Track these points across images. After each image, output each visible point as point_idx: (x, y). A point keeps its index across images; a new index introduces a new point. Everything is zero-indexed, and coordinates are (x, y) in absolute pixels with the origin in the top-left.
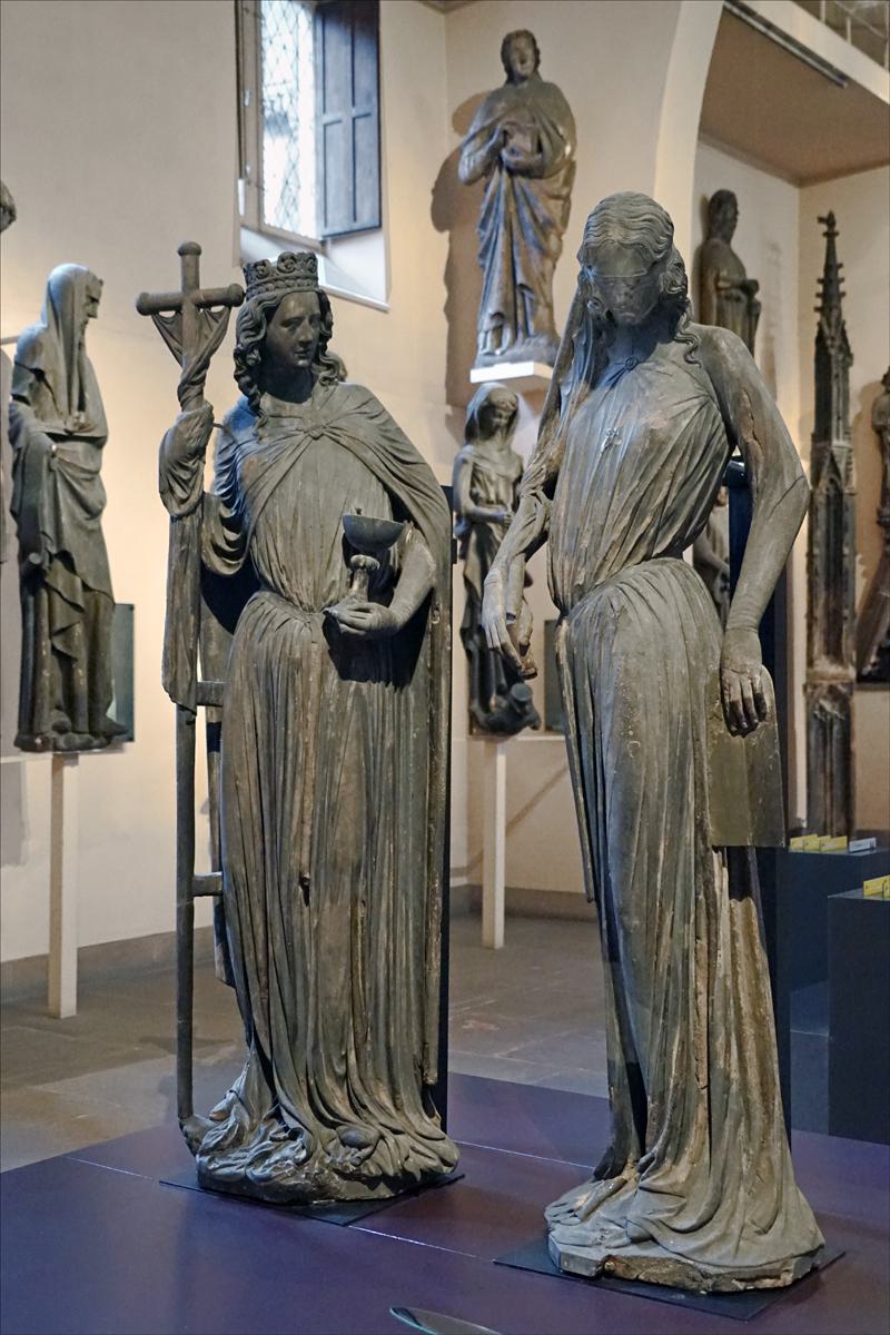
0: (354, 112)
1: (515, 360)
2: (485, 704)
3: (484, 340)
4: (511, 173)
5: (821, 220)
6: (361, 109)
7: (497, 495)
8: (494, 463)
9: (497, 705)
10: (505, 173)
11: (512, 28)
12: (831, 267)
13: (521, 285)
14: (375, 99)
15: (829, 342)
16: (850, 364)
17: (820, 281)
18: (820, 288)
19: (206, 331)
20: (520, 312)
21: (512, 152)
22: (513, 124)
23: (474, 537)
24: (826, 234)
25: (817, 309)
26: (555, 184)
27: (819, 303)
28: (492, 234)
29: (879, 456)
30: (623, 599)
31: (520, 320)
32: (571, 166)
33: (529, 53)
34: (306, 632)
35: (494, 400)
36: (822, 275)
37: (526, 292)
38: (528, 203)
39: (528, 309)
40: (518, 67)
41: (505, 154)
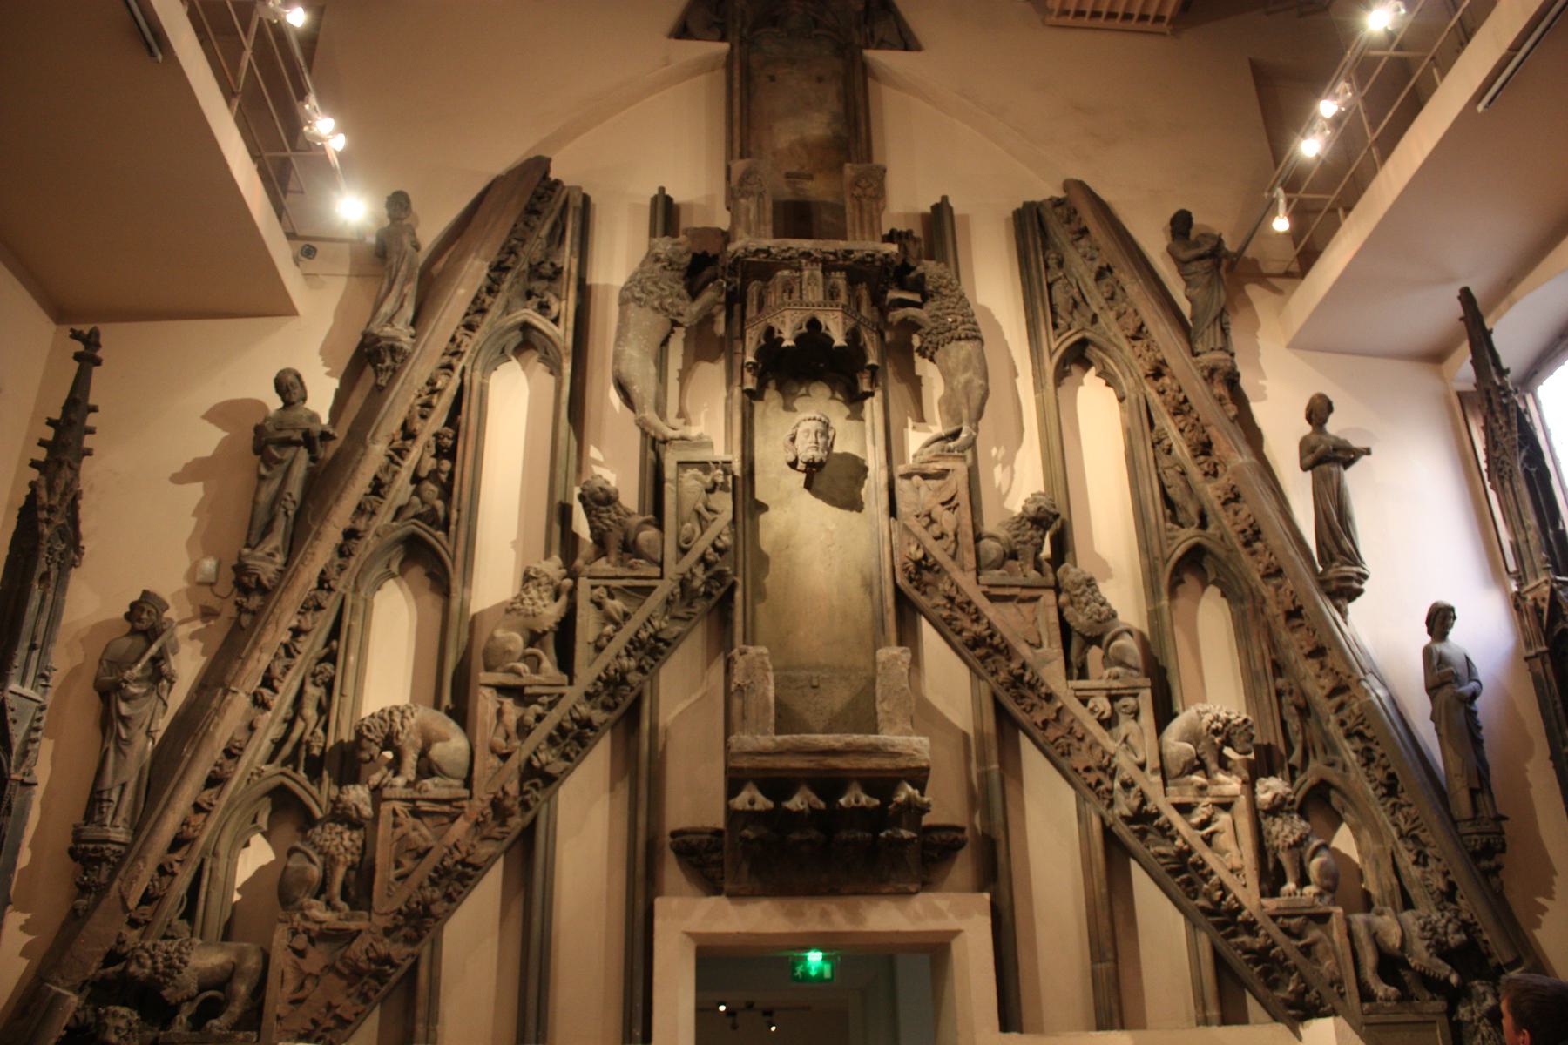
12: (76, 408)
15: (43, 515)
16: (74, 564)
17: (51, 423)
24: (78, 357)
25: (34, 464)
27: (41, 454)
29: (96, 735)
36: (57, 415)
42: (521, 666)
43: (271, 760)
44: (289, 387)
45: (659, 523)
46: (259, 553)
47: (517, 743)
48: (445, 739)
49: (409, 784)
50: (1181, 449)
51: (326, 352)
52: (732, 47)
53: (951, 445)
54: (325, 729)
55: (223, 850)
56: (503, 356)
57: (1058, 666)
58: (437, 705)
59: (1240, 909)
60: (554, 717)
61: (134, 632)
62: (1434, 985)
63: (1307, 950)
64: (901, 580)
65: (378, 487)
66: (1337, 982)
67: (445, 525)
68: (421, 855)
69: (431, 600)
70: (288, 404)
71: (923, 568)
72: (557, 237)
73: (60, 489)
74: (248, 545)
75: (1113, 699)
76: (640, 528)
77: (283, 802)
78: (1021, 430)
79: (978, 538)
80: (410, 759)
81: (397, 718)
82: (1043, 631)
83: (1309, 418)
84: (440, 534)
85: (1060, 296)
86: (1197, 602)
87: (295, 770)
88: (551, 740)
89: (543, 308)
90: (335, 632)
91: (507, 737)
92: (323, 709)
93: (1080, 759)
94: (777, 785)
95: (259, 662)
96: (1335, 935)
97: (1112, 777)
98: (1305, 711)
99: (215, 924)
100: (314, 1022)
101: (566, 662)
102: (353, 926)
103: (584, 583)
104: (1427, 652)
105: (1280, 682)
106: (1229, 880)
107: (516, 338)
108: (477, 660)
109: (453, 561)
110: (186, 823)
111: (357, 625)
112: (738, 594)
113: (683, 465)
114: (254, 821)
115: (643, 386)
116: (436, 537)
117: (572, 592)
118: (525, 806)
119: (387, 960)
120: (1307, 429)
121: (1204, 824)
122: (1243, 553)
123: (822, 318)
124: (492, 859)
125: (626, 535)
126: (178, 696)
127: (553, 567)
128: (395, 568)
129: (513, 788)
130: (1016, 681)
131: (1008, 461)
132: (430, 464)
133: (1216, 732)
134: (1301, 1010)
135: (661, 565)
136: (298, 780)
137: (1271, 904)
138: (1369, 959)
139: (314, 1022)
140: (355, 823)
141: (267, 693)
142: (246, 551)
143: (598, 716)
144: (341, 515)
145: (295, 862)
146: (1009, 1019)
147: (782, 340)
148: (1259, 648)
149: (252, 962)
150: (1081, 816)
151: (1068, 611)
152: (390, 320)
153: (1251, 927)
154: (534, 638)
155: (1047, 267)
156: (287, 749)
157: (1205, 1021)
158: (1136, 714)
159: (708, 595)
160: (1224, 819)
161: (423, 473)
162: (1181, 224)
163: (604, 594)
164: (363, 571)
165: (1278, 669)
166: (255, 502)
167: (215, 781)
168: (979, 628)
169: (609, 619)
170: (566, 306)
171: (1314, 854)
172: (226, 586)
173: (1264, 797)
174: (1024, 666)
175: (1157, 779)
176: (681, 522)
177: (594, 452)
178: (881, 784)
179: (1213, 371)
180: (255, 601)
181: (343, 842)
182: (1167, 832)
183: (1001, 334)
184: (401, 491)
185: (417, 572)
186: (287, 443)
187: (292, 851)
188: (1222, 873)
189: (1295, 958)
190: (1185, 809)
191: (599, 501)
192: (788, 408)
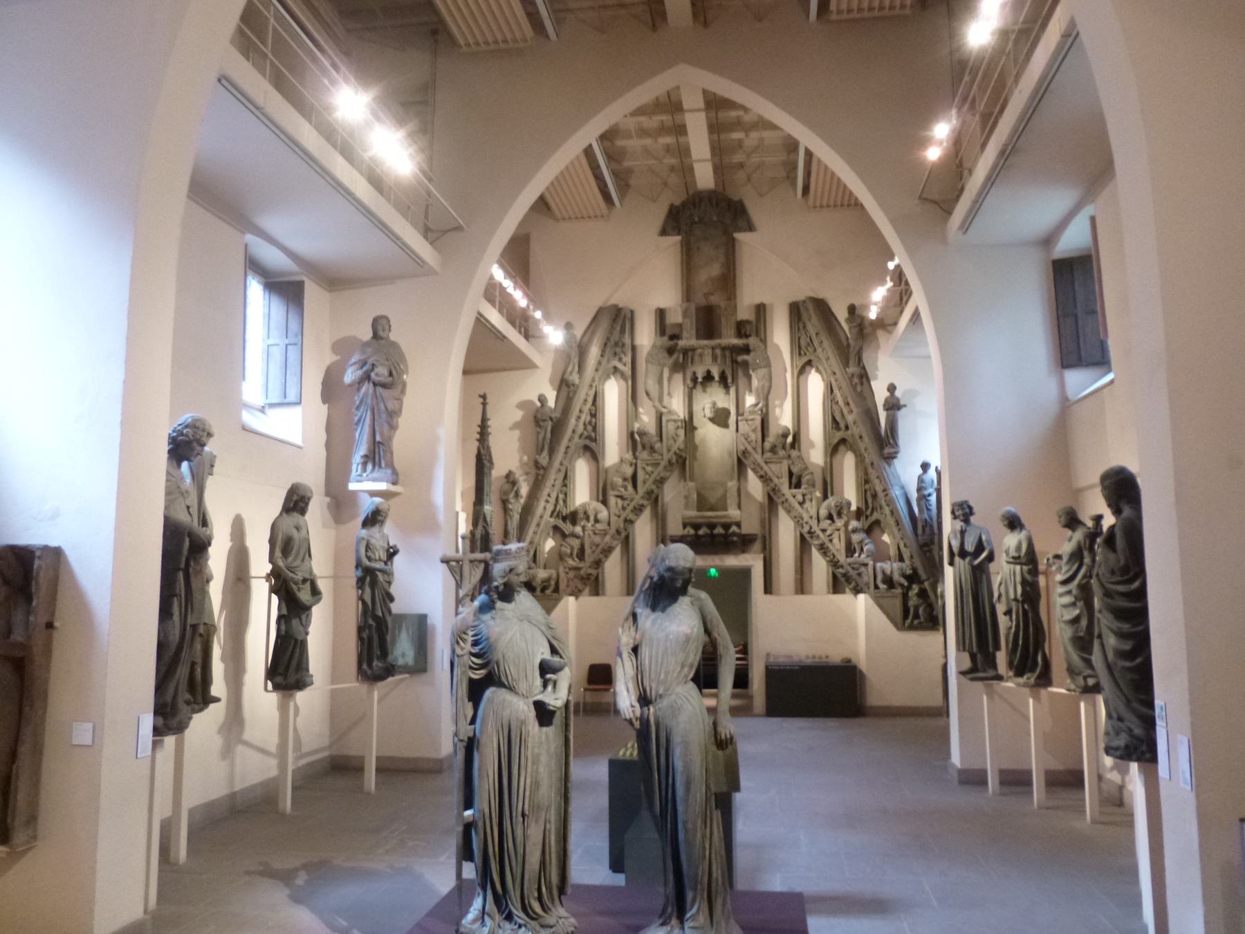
0: (287, 341)
1: (374, 480)
2: (370, 665)
3: (356, 468)
4: (375, 384)
5: (480, 396)
6: (292, 339)
7: (379, 557)
8: (377, 539)
9: (377, 666)
10: (371, 384)
11: (379, 313)
12: (484, 420)
13: (379, 442)
14: (300, 337)
15: (484, 457)
17: (479, 426)
18: (479, 430)
19: (473, 572)
20: (377, 456)
21: (377, 375)
22: (378, 361)
23: (368, 579)
26: (394, 392)
28: (363, 413)
29: (502, 515)
30: (681, 701)
31: (377, 460)
32: (404, 385)
33: (387, 327)
34: (526, 708)
35: (380, 508)
36: (480, 423)
37: (381, 445)
38: (384, 402)
39: (382, 454)
40: (381, 333)
41: (373, 375)
42: (622, 490)
43: (551, 516)
44: (542, 399)
45: (661, 440)
46: (542, 456)
47: (622, 512)
48: (601, 512)
49: (592, 526)
50: (841, 403)
51: (551, 381)
52: (683, 238)
53: (756, 409)
54: (566, 507)
55: (541, 544)
56: (608, 377)
57: (787, 485)
58: (598, 500)
59: (839, 561)
60: (632, 504)
61: (508, 482)
62: (902, 585)
63: (859, 575)
64: (739, 455)
65: (574, 431)
66: (867, 584)
67: (595, 440)
68: (597, 546)
69: (593, 463)
70: (542, 405)
71: (745, 452)
72: (622, 331)
73: (486, 448)
74: (537, 454)
75: (804, 495)
76: (655, 443)
77: (556, 528)
78: (786, 393)
79: (763, 440)
80: (592, 518)
81: (587, 506)
82: (783, 471)
83: (888, 390)
84: (594, 444)
85: (803, 342)
86: (844, 455)
87: (559, 519)
88: (632, 511)
89: (620, 360)
90: (565, 477)
91: (619, 511)
92: (565, 501)
93: (793, 514)
94: (697, 527)
95: (546, 491)
96: (869, 570)
97: (803, 519)
98: (875, 496)
99: (542, 565)
100: (573, 591)
101: (635, 486)
102: (581, 565)
103: (639, 462)
104: (919, 477)
105: (867, 486)
106: (836, 553)
107: (612, 370)
108: (609, 487)
109: (599, 452)
110: (532, 538)
111: (572, 475)
112: (687, 462)
113: (668, 421)
114: (549, 534)
115: (654, 392)
116: (593, 445)
117: (636, 465)
118: (626, 530)
119: (590, 574)
120: (888, 394)
121: (830, 535)
122: (859, 440)
123: (711, 370)
124: (617, 545)
125: (651, 445)
126: (522, 501)
127: (629, 456)
128: (581, 454)
129: (622, 525)
130: (774, 490)
131: (781, 406)
132: (589, 418)
133: (837, 506)
134: (857, 591)
135: (662, 455)
136: (560, 523)
137: (849, 560)
138: (880, 577)
139: (573, 591)
140: (578, 537)
141: (548, 498)
142: (537, 457)
143: (645, 502)
144: (564, 443)
145: (563, 549)
146: (768, 589)
147: (697, 378)
148: (862, 474)
149: (554, 576)
150: (795, 530)
151: (792, 468)
152: (571, 373)
153: (842, 567)
154: (625, 479)
155: (799, 329)
156: (555, 514)
157: (829, 593)
158: (811, 500)
159: (677, 462)
160: (837, 533)
161: (587, 423)
162: (852, 309)
163: (644, 465)
164: (572, 456)
165: (867, 481)
166: (538, 440)
167: (538, 525)
168: (762, 473)
169: (647, 473)
170: (628, 359)
171: (866, 545)
172: (532, 464)
173: (850, 528)
174: (776, 485)
175: (816, 521)
176: (668, 439)
177: (641, 410)
178: (726, 526)
179: (853, 375)
180: (541, 472)
181: (576, 543)
182: (818, 537)
183: (782, 354)
184: (581, 427)
185: (588, 454)
186: (544, 420)
187: (562, 545)
188: (833, 550)
189: (857, 577)
190: (824, 531)
191: (642, 434)
192: (704, 391)
